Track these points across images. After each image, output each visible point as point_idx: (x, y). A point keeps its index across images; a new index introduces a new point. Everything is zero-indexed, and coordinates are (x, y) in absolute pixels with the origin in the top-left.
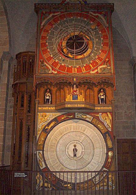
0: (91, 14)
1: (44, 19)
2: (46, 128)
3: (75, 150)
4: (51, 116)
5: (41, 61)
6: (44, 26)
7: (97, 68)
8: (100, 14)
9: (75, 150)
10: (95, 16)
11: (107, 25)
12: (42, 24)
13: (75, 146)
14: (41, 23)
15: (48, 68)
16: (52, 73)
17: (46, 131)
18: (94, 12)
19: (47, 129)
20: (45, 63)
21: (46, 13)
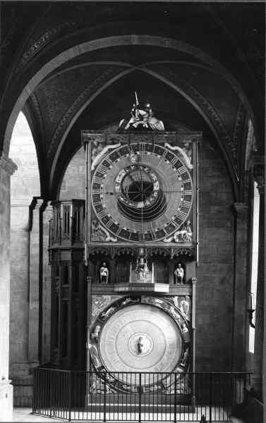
0: (167, 147)
1: (96, 154)
2: (103, 315)
3: (139, 345)
4: (109, 299)
5: (94, 223)
6: (96, 167)
7: (173, 235)
8: (182, 147)
9: (139, 345)
10: (173, 151)
11: (191, 167)
12: (94, 164)
13: (140, 339)
14: (92, 161)
15: (105, 234)
16: (110, 241)
17: (102, 320)
18: (172, 145)
19: (103, 317)
20: (100, 226)
21: (98, 143)
